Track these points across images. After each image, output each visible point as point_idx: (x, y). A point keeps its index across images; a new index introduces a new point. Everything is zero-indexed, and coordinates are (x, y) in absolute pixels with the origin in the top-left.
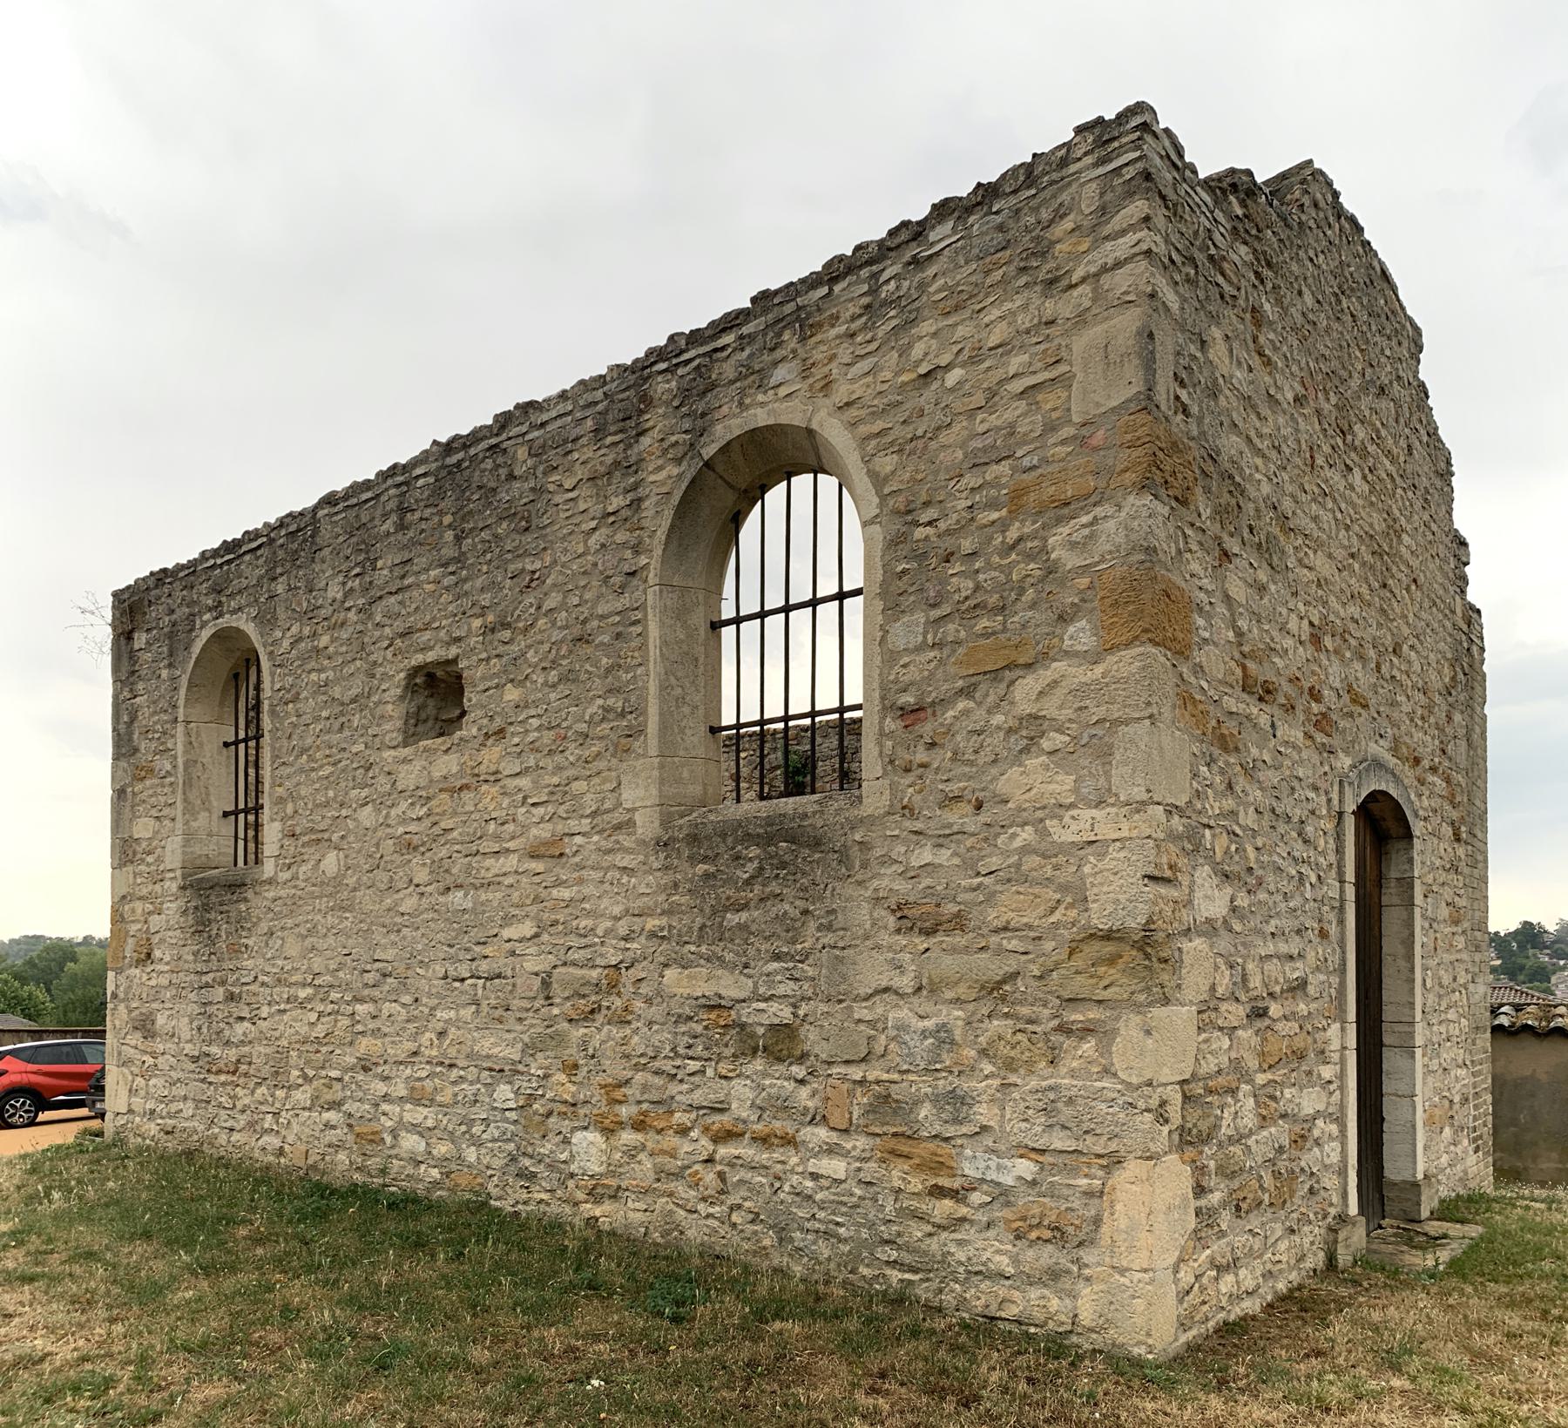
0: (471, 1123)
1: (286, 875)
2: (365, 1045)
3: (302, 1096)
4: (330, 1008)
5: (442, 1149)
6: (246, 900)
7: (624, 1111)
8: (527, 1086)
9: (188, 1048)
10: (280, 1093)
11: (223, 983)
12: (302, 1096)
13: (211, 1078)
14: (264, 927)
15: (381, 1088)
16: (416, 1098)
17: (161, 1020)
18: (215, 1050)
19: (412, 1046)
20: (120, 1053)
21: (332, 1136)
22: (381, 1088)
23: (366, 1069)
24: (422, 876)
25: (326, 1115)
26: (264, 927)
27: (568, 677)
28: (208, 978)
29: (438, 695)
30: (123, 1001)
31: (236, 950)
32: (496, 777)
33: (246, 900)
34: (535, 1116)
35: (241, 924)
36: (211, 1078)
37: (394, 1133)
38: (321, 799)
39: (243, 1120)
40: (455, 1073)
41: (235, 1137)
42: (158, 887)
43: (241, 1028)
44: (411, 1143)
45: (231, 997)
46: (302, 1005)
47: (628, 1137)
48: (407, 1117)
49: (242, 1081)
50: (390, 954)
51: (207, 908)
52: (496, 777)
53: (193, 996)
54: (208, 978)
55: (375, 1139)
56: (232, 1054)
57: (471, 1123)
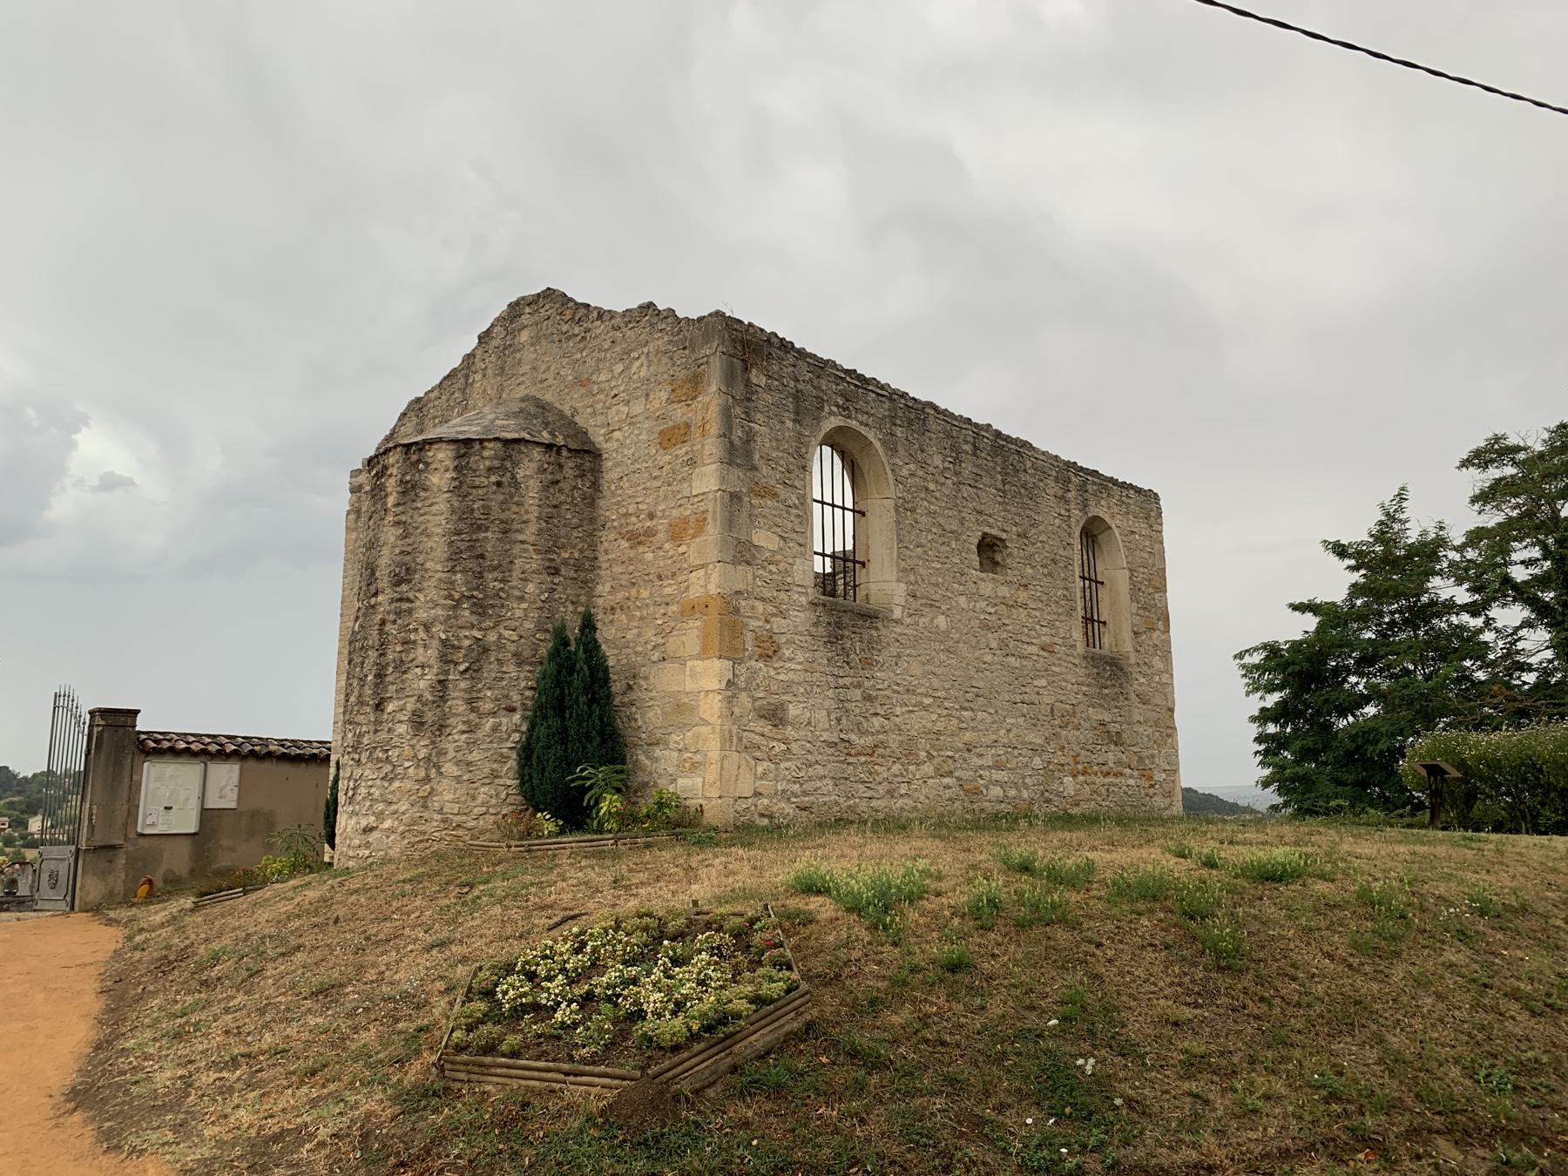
0: (1024, 777)
1: (908, 621)
2: (968, 736)
3: (928, 769)
4: (945, 712)
5: (1012, 793)
6: (877, 629)
7: (1080, 767)
8: (1046, 757)
9: (826, 736)
10: (912, 768)
11: (859, 686)
12: (928, 769)
13: (851, 760)
14: (894, 650)
15: (976, 761)
16: (998, 766)
17: (793, 711)
18: (853, 737)
19: (994, 737)
20: (740, 739)
21: (948, 794)
22: (976, 761)
23: (969, 750)
24: (994, 645)
25: (946, 780)
26: (894, 650)
27: (1050, 574)
28: (847, 681)
29: (989, 549)
30: (744, 689)
31: (868, 663)
32: (1024, 606)
33: (877, 629)
34: (1049, 772)
35: (872, 644)
36: (851, 760)
37: (987, 788)
38: (933, 580)
39: (881, 790)
40: (1016, 752)
41: (874, 803)
42: (783, 595)
43: (877, 722)
44: (996, 791)
45: (868, 698)
46: (925, 708)
47: (1081, 778)
48: (994, 777)
49: (879, 760)
50: (981, 684)
51: (839, 625)
52: (1024, 606)
53: (830, 693)
54: (847, 681)
55: (976, 792)
56: (868, 741)
57: (1024, 777)
